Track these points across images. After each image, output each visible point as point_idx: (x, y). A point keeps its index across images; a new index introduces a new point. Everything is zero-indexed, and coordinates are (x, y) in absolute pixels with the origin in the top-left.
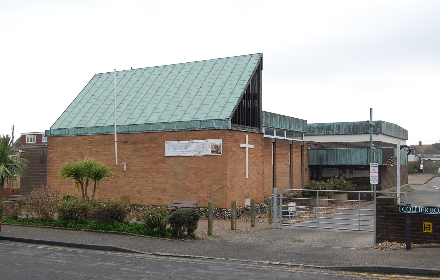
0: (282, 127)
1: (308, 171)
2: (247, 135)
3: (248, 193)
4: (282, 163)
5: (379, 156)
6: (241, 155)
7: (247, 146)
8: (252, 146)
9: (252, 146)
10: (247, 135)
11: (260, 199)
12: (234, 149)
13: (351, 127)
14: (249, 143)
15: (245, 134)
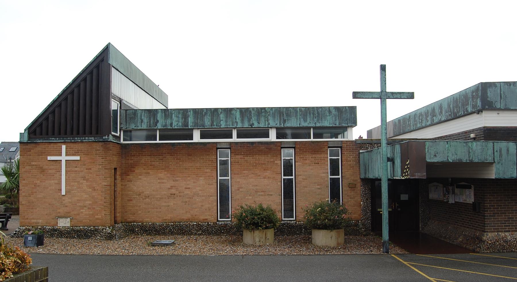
0: (253, 124)
1: (359, 187)
2: (64, 147)
3: (69, 213)
4: (253, 175)
5: (398, 159)
6: (50, 169)
7: (64, 158)
8: (78, 158)
9: (78, 158)
10: (64, 147)
11: (98, 221)
12: (33, 163)
13: (451, 106)
14: (67, 155)
15: (59, 144)
